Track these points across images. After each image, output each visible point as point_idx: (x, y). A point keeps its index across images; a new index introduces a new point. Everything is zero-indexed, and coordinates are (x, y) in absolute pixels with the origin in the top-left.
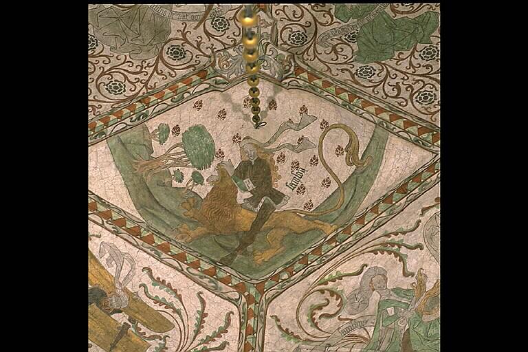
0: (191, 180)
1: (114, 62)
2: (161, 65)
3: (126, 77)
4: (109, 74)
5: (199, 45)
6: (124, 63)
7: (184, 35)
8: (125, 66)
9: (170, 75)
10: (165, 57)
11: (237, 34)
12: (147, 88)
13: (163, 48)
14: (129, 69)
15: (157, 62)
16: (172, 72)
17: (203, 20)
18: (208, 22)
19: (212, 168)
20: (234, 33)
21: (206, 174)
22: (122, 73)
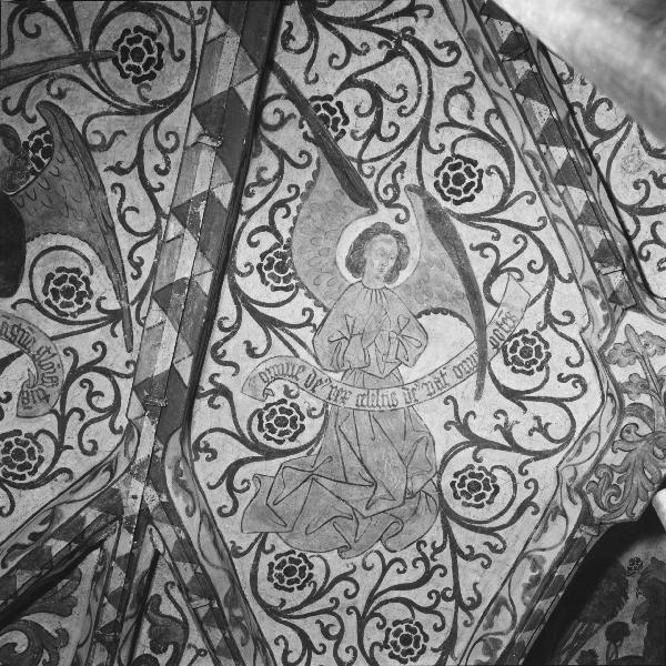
0: (609, 647)
1: (367, 581)
2: (462, 536)
3: (409, 604)
4: (373, 615)
5: (508, 436)
6: (385, 569)
7: (463, 428)
8: (392, 578)
9: (493, 549)
10: (457, 507)
11: (575, 359)
12: (466, 609)
13: (439, 489)
14: (403, 579)
15: (447, 531)
16: (494, 540)
17: (483, 365)
18: (497, 364)
19: (631, 596)
20: (568, 361)
21: (625, 615)
22: (393, 600)
